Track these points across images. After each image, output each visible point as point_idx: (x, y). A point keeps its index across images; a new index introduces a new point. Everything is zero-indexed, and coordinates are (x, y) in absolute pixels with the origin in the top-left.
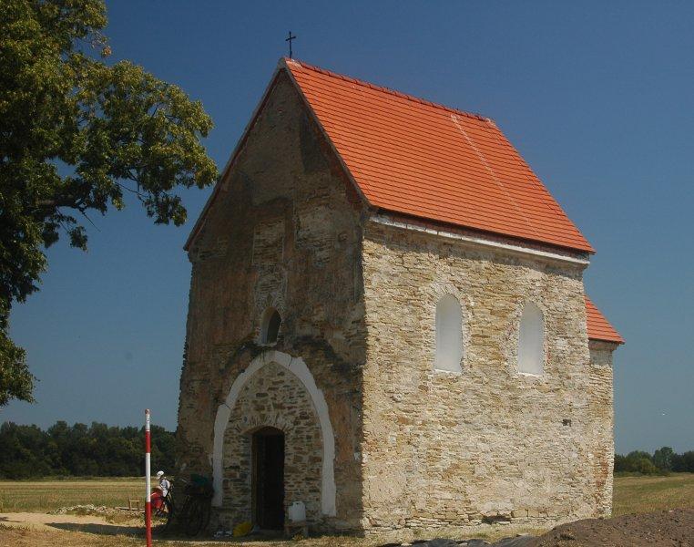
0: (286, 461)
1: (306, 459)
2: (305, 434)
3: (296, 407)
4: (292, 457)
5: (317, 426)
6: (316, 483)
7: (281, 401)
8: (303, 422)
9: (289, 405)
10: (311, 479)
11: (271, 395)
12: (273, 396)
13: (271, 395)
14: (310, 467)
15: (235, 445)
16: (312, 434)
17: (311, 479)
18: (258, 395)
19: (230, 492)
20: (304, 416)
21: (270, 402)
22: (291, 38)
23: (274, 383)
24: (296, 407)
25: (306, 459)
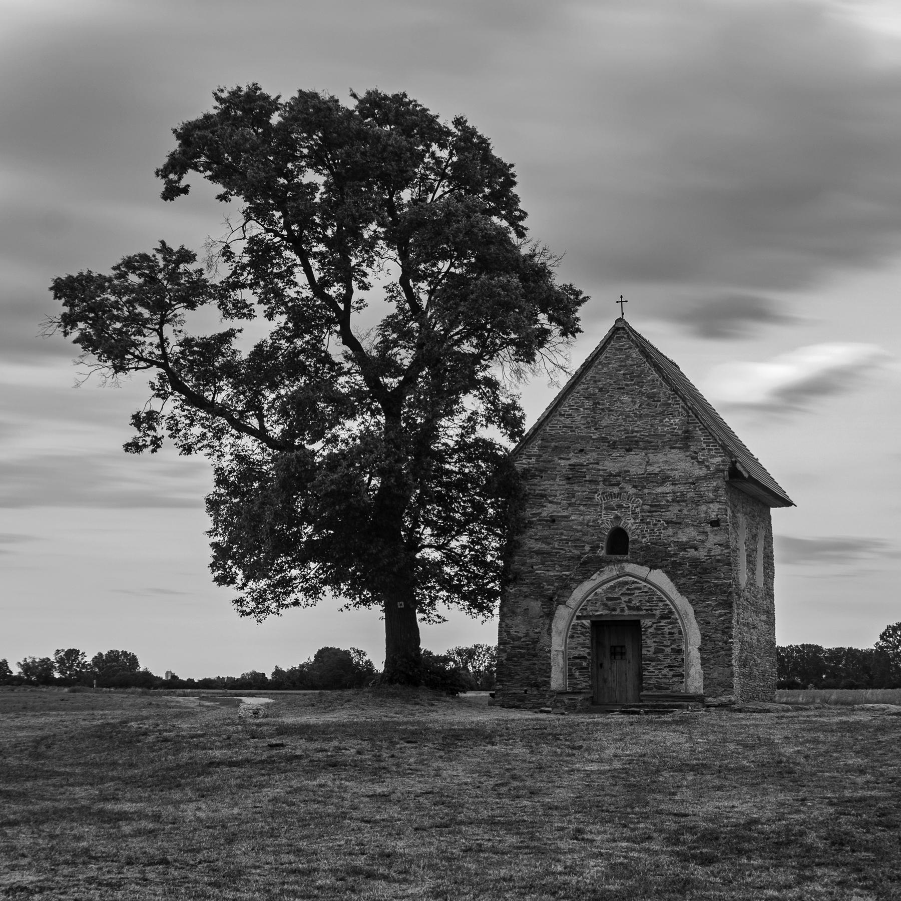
0: (644, 652)
4: (652, 649)
23: (628, 589)
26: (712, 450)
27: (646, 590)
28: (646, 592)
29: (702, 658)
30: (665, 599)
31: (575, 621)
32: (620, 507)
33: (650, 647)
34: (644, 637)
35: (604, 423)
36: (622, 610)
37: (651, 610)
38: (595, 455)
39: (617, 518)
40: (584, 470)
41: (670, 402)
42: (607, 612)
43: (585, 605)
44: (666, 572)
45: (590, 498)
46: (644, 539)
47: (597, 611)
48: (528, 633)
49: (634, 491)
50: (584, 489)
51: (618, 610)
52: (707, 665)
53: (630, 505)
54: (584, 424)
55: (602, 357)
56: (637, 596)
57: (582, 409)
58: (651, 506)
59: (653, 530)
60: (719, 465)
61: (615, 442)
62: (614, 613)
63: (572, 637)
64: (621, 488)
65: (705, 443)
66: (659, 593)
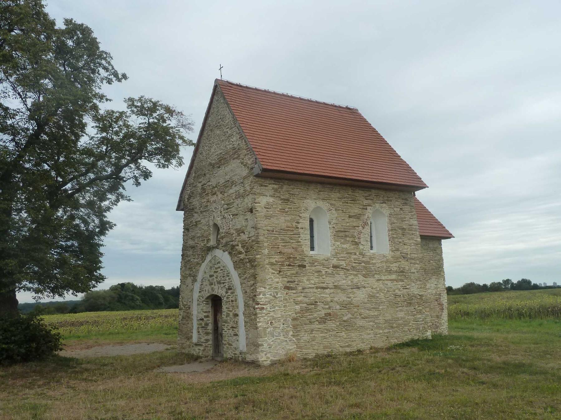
0: (223, 316)
3: (226, 283)
5: (236, 294)
8: (230, 291)
9: (223, 282)
11: (215, 275)
13: (215, 275)
20: (230, 289)
24: (226, 283)
25: (231, 314)
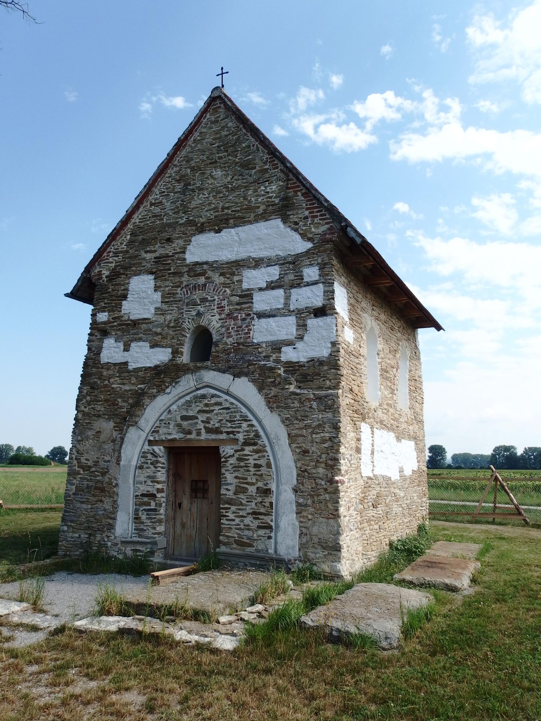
0: (223, 491)
1: (252, 490)
2: (252, 462)
4: (232, 488)
6: (267, 519)
7: (217, 425)
10: (261, 514)
12: (204, 419)
13: (202, 417)
14: (260, 499)
15: (148, 470)
16: (262, 462)
17: (261, 514)
18: (184, 418)
19: (143, 523)
21: (201, 426)
22: (222, 74)
23: (206, 405)
24: (239, 432)
25: (252, 490)
26: (316, 216)
27: (227, 405)
28: (228, 409)
29: (298, 504)
30: (251, 417)
31: (146, 447)
32: (204, 300)
33: (231, 484)
34: (223, 471)
35: (193, 204)
36: (199, 434)
37: (233, 432)
38: (181, 242)
39: (199, 314)
40: (170, 262)
41: (266, 167)
42: (182, 436)
43: (157, 427)
44: (253, 381)
45: (173, 294)
46: (231, 339)
47: (170, 434)
48: (98, 462)
49: (222, 279)
50: (167, 283)
51: (194, 432)
52: (304, 514)
53: (216, 297)
54: (172, 210)
55: (196, 135)
56: (217, 414)
57: (172, 194)
58: (240, 296)
59: (241, 327)
60: (325, 234)
61: (203, 224)
62: (189, 436)
63: (141, 467)
64: (207, 278)
65: (307, 209)
66: (244, 410)
